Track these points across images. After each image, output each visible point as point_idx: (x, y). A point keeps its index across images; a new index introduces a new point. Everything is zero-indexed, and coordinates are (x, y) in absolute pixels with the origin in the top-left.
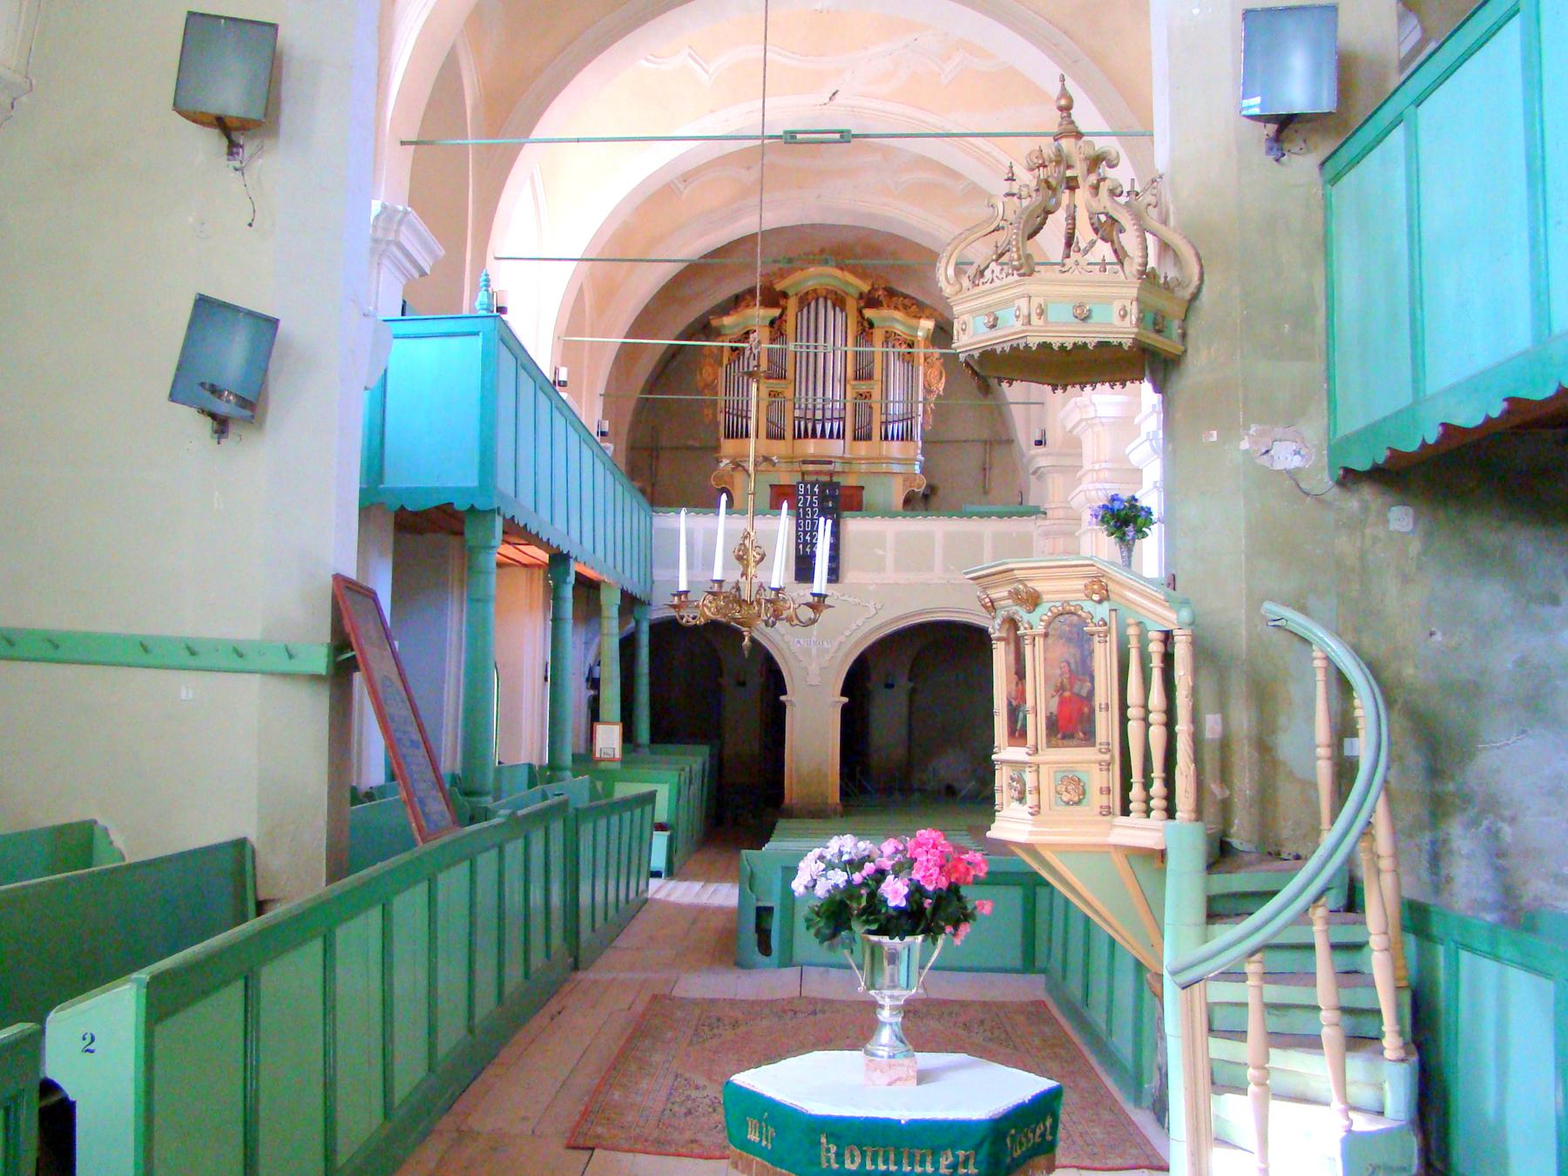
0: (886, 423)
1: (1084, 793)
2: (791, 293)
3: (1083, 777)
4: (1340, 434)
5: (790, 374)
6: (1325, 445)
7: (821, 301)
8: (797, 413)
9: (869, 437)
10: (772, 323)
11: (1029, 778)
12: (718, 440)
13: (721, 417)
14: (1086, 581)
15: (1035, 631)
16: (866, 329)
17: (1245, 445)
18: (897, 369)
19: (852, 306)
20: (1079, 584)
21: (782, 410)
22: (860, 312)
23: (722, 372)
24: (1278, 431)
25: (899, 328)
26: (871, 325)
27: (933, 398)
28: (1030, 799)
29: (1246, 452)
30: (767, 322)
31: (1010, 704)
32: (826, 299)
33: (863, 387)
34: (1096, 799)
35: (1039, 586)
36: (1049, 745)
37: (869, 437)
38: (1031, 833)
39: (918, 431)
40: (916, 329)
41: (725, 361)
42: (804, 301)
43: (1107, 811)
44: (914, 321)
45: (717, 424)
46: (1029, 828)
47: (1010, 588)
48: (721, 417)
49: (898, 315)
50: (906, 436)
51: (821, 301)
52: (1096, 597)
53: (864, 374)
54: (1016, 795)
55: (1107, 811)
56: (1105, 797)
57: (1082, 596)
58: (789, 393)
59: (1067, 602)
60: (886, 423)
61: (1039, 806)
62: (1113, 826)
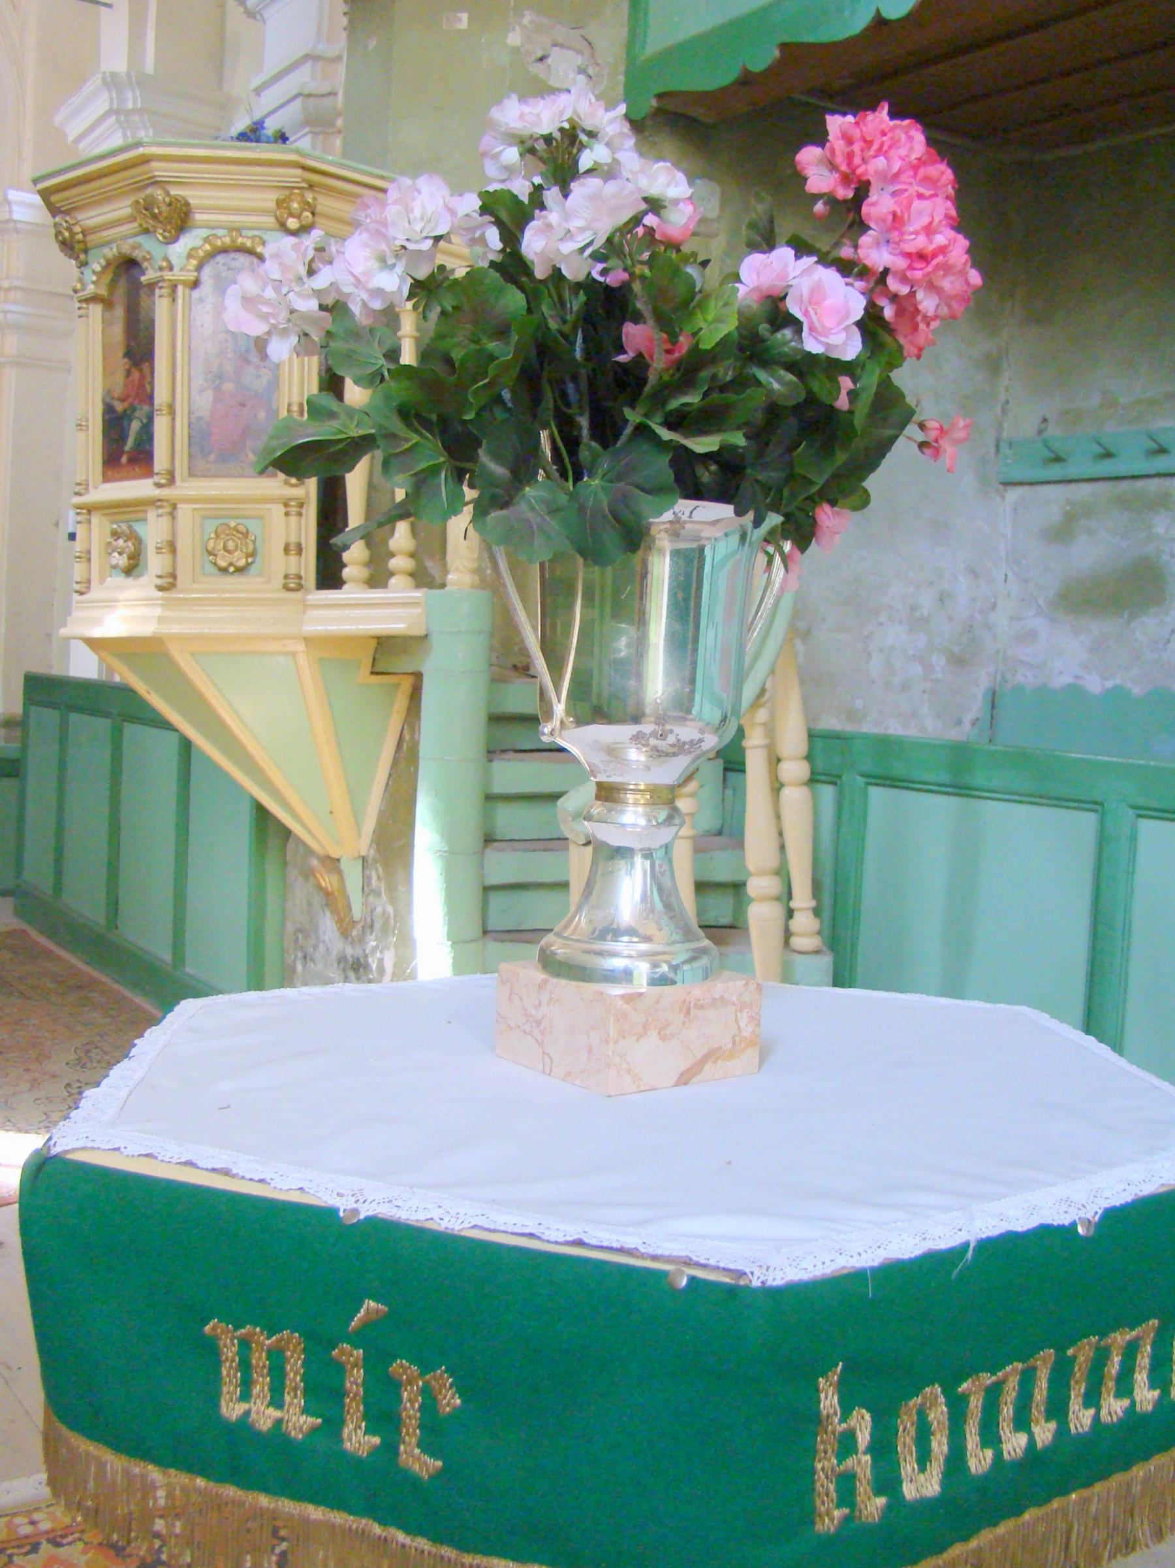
1: (253, 554)
3: (253, 526)
4: (649, 51)
6: (622, 69)
11: (153, 530)
14: (280, 194)
15: (176, 275)
17: (514, 39)
20: (269, 199)
24: (561, 32)
28: (155, 563)
29: (516, 50)
31: (109, 409)
34: (278, 564)
35: (194, 196)
36: (192, 473)
38: (160, 620)
43: (293, 584)
46: (158, 611)
47: (140, 196)
52: (292, 223)
54: (123, 561)
55: (293, 584)
56: (293, 559)
57: (270, 221)
59: (239, 230)
61: (174, 576)
62: (306, 606)
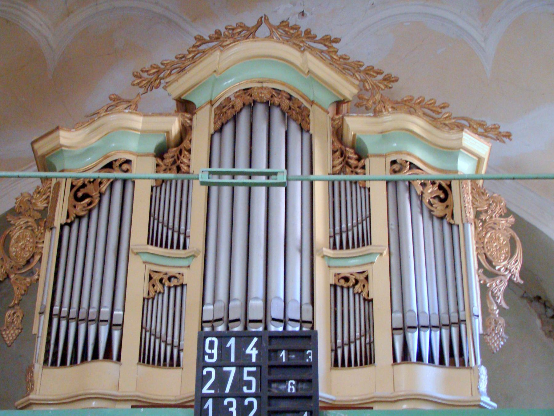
0: (403, 329)
2: (198, 100)
5: (196, 241)
7: (260, 110)
8: (209, 312)
9: (368, 359)
10: (160, 153)
12: (30, 369)
13: (40, 326)
16: (350, 155)
18: (419, 232)
19: (320, 123)
21: (177, 318)
22: (338, 133)
23: (50, 242)
25: (418, 154)
26: (361, 155)
27: (499, 287)
30: (151, 146)
32: (269, 106)
33: (351, 262)
37: (368, 359)
39: (473, 351)
40: (451, 152)
41: (60, 218)
42: (227, 116)
44: (445, 137)
45: (35, 337)
48: (40, 326)
49: (417, 124)
50: (452, 357)
51: (260, 110)
53: (351, 236)
58: (192, 278)
60: (403, 329)
